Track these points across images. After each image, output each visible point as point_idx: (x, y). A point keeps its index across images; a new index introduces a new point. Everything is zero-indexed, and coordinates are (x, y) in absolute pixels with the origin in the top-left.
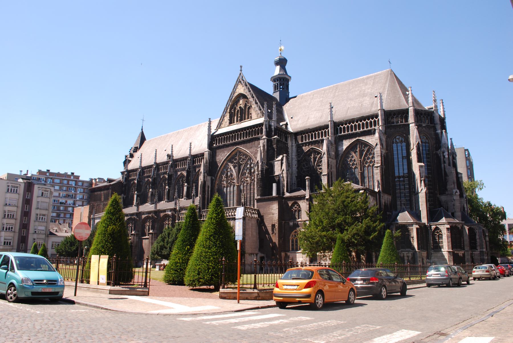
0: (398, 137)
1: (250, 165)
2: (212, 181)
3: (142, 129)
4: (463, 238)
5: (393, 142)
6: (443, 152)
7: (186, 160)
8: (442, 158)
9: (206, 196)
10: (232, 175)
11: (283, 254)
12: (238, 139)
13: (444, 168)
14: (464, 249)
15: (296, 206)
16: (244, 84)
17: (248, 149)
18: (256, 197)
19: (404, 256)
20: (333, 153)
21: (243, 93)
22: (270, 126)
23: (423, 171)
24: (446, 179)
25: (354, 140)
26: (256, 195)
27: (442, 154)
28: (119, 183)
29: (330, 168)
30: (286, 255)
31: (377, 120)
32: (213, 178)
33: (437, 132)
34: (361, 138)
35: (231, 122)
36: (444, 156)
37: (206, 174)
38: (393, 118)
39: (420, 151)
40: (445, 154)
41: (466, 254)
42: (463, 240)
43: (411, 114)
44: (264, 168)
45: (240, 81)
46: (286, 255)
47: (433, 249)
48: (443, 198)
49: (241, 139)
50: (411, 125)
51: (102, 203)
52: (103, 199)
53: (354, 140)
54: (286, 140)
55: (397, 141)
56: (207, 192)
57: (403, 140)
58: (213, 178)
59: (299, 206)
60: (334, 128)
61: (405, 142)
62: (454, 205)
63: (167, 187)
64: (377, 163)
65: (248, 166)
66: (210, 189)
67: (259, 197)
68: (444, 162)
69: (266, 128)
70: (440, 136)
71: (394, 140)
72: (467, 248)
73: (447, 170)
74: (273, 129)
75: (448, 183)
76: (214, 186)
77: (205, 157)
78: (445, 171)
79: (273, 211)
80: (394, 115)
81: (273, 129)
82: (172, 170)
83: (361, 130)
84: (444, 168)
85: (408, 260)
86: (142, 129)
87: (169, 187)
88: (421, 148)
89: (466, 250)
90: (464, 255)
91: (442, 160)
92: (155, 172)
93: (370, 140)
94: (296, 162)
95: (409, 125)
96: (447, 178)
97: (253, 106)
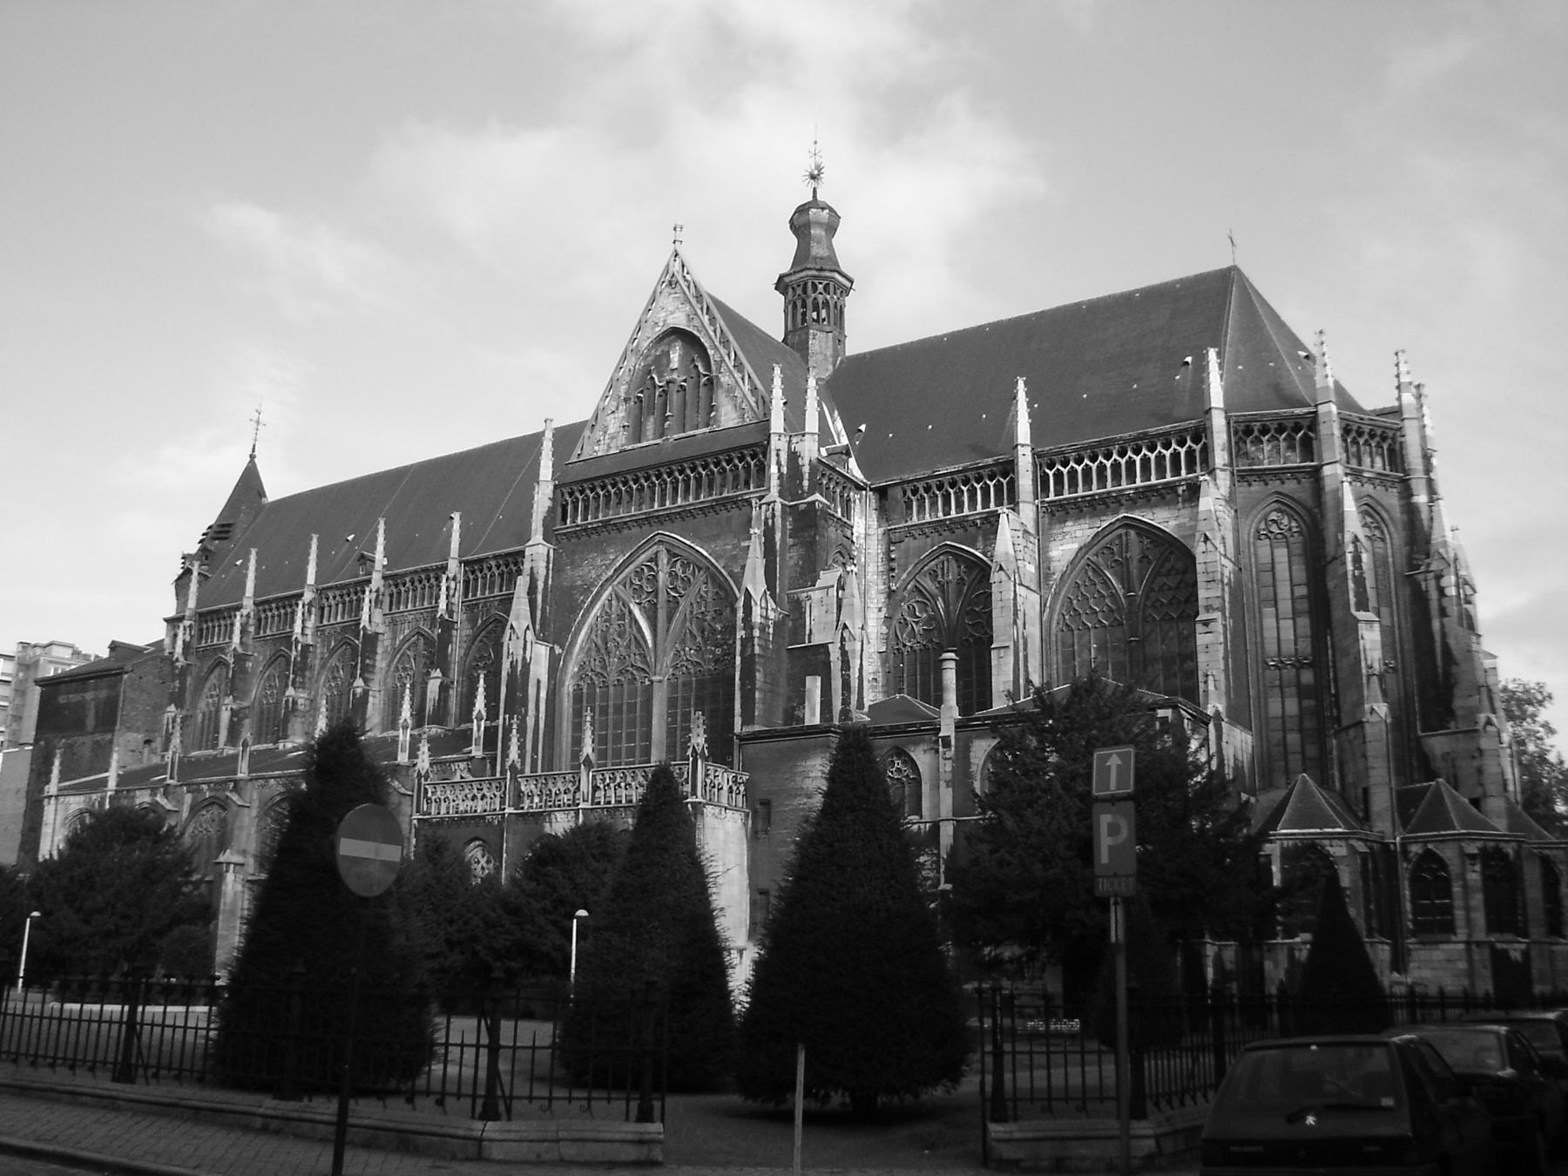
3: (252, 457)
4: (1523, 891)
6: (1439, 577)
7: (438, 579)
8: (1434, 595)
9: (530, 722)
13: (1444, 635)
14: (1526, 936)
16: (691, 294)
17: (703, 541)
18: (737, 729)
20: (1032, 568)
21: (683, 325)
22: (794, 456)
23: (1373, 642)
24: (1448, 674)
27: (1432, 583)
29: (1020, 622)
31: (1197, 448)
32: (558, 650)
33: (1415, 499)
36: (1441, 591)
37: (530, 636)
38: (1258, 441)
40: (1444, 582)
41: (1534, 953)
42: (1524, 901)
43: (1331, 430)
44: (772, 615)
47: (1414, 934)
48: (1438, 744)
50: (1327, 470)
51: (88, 740)
52: (90, 722)
54: (847, 512)
56: (531, 706)
58: (558, 650)
60: (1035, 473)
62: (1480, 771)
63: (359, 682)
64: (1208, 608)
66: (543, 694)
67: (748, 729)
68: (1443, 612)
69: (779, 464)
70: (1424, 515)
71: (1263, 526)
72: (1537, 931)
73: (1452, 642)
74: (806, 469)
75: (1458, 692)
77: (527, 566)
78: (1445, 645)
80: (1264, 430)
81: (806, 469)
82: (378, 616)
83: (1139, 483)
84: (1444, 635)
86: (252, 457)
87: (366, 681)
88: (1365, 557)
89: (1535, 937)
90: (1526, 954)
91: (1434, 605)
92: (310, 624)
94: (882, 598)
96: (1454, 669)
97: (725, 379)
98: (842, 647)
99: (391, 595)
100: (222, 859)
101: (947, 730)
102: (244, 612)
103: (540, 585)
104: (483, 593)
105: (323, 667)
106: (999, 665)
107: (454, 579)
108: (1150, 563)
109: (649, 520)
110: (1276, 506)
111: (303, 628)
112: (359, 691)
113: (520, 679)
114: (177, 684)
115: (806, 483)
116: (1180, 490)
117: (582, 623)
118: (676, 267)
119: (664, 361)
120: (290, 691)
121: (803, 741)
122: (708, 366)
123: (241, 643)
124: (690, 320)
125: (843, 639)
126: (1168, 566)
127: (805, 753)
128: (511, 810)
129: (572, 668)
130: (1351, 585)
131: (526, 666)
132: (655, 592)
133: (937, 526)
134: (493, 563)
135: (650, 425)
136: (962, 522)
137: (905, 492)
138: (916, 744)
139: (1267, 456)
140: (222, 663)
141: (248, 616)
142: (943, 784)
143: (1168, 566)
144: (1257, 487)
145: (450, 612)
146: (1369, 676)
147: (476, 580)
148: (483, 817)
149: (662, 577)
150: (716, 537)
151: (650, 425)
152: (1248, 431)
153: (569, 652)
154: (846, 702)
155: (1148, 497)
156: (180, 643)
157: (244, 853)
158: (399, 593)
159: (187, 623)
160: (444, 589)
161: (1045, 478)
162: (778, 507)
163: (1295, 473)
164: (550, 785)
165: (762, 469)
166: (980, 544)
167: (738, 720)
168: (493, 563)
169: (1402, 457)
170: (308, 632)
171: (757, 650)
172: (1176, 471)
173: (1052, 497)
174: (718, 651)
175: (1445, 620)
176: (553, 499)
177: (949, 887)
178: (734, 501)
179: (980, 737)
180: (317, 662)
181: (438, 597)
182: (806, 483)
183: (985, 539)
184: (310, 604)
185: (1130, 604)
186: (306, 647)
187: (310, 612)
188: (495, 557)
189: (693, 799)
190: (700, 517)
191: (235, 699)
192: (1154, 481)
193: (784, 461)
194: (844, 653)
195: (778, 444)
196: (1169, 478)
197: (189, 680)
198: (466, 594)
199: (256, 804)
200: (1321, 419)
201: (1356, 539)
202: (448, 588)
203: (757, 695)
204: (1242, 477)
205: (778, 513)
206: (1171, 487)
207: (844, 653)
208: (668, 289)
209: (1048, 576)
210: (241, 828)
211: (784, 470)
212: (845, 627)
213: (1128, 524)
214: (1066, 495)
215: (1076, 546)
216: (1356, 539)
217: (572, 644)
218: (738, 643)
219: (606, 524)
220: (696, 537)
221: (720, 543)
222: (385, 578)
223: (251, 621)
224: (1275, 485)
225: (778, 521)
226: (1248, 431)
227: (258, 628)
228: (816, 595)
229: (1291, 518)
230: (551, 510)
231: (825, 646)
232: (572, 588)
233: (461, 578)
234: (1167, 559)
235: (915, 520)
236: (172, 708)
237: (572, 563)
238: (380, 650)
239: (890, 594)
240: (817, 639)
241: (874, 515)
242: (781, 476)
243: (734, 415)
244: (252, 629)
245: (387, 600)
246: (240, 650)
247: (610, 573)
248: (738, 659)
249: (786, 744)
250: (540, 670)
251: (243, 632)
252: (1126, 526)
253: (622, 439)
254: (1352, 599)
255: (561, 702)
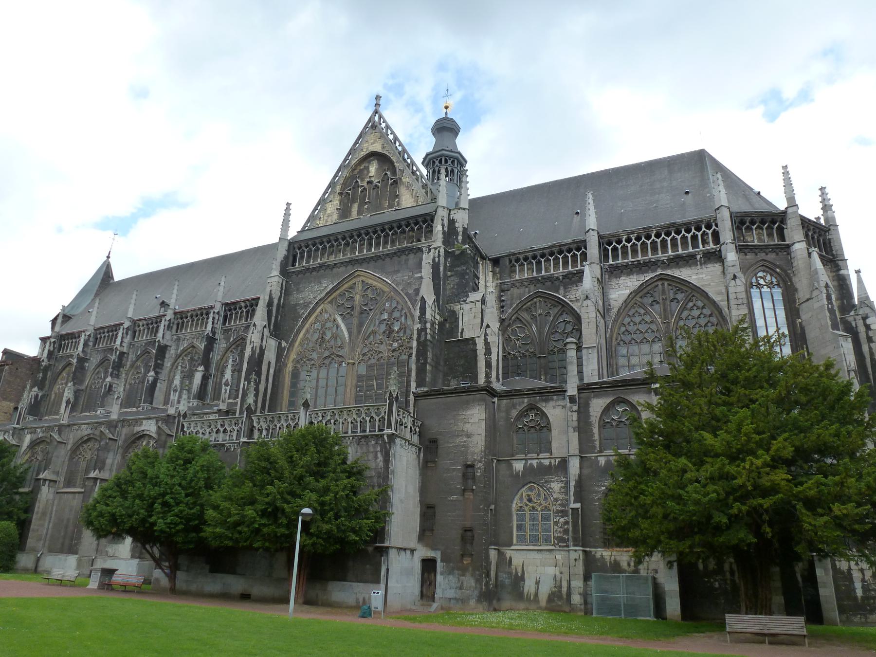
0: (760, 274)
1: (390, 314)
2: (280, 351)
3: (108, 257)
5: (751, 283)
7: (208, 314)
8: (862, 329)
10: (335, 336)
11: (493, 554)
12: (361, 251)
15: (532, 415)
17: (388, 274)
19: (850, 569)
22: (452, 222)
25: (649, 276)
26: (413, 385)
27: (860, 323)
28: (36, 360)
30: (501, 554)
32: (284, 344)
34: (669, 272)
35: (344, 212)
38: (749, 229)
39: (832, 304)
45: (374, 125)
46: (501, 554)
49: (369, 250)
53: (649, 276)
55: (762, 282)
56: (263, 377)
57: (774, 280)
58: (284, 344)
59: (544, 414)
60: (600, 247)
61: (778, 285)
63: (152, 373)
65: (386, 316)
66: (272, 371)
67: (420, 390)
69: (443, 225)
71: (754, 280)
76: (285, 365)
79: (468, 427)
80: (753, 223)
81: (460, 230)
85: (863, 580)
86: (108, 257)
87: (157, 373)
93: (694, 277)
95: (788, 247)
98: (486, 340)
99: (178, 324)
100: (41, 476)
101: (572, 389)
102: (88, 333)
103: (276, 302)
104: (235, 322)
105: (132, 366)
106: (588, 359)
107: (218, 313)
108: (678, 302)
109: (352, 262)
110: (762, 268)
111: (122, 342)
112: (151, 379)
113: (257, 361)
114: (41, 375)
115: (460, 238)
116: (698, 257)
117: (302, 327)
118: (376, 118)
119: (366, 172)
120: (109, 379)
121: (465, 397)
122: (394, 172)
123: (83, 351)
124: (383, 148)
125: (486, 335)
126: (691, 304)
127: (467, 405)
128: (245, 440)
129: (293, 356)
130: (828, 314)
131: (262, 351)
132: (352, 308)
133: (533, 281)
134: (243, 305)
135: (355, 208)
136: (550, 278)
137: (511, 261)
138: (547, 401)
139: (754, 238)
140: (69, 364)
141: (89, 336)
142: (571, 430)
143: (691, 304)
144: (750, 256)
145: (213, 332)
146: (849, 371)
147: (231, 315)
148: (223, 445)
149: (357, 298)
150: (398, 271)
151: (355, 208)
152: (742, 223)
153: (292, 345)
154: (488, 376)
155: (678, 261)
156: (46, 351)
157: (57, 473)
158: (183, 323)
159: (52, 340)
160: (211, 319)
161: (606, 250)
162: (442, 250)
163: (775, 249)
164: (276, 422)
165: (430, 229)
166: (562, 291)
167: (413, 385)
168: (243, 305)
169: (831, 247)
170: (124, 344)
171: (429, 337)
172: (695, 246)
173: (611, 262)
174: (395, 345)
175: (872, 345)
176: (288, 251)
177: (578, 505)
178: (411, 250)
179: (596, 397)
180: (129, 363)
181: (207, 323)
182: (460, 238)
183: (565, 288)
184: (128, 329)
185: (668, 327)
186: (122, 354)
187: (127, 333)
188: (245, 301)
189: (389, 431)
190: (388, 260)
191: (74, 385)
192: (680, 251)
193: (446, 224)
194: (487, 344)
195: (442, 213)
196: (691, 250)
197: (49, 373)
198: (224, 323)
199: (71, 442)
200: (789, 216)
201: (827, 286)
202: (214, 318)
203: (428, 367)
204: (742, 249)
205: (442, 254)
206: (692, 256)
207: (487, 344)
208: (371, 131)
209: (609, 310)
210: (58, 457)
211: (446, 229)
212: (488, 326)
213: (662, 278)
214: (620, 261)
215: (628, 292)
216: (827, 286)
217: (294, 341)
218: (415, 332)
219: (322, 266)
220: (383, 270)
221: (399, 275)
222: (175, 314)
223: (91, 339)
224: (762, 256)
225: (442, 259)
226: (742, 223)
227: (94, 345)
228: (466, 307)
229: (771, 275)
230: (286, 258)
231: (472, 341)
232: (296, 305)
233: (222, 313)
234: (690, 300)
235: (517, 277)
236: (36, 389)
237: (298, 290)
238: (167, 356)
239: (502, 321)
240: (467, 335)
241: (491, 274)
242: (444, 233)
243: (411, 200)
244: (91, 344)
245: (175, 327)
246: (81, 355)
247: (323, 295)
248: (415, 344)
249: (450, 399)
250: (270, 356)
251: (86, 344)
252: (661, 279)
253: (335, 217)
254: (830, 323)
255: (284, 377)
